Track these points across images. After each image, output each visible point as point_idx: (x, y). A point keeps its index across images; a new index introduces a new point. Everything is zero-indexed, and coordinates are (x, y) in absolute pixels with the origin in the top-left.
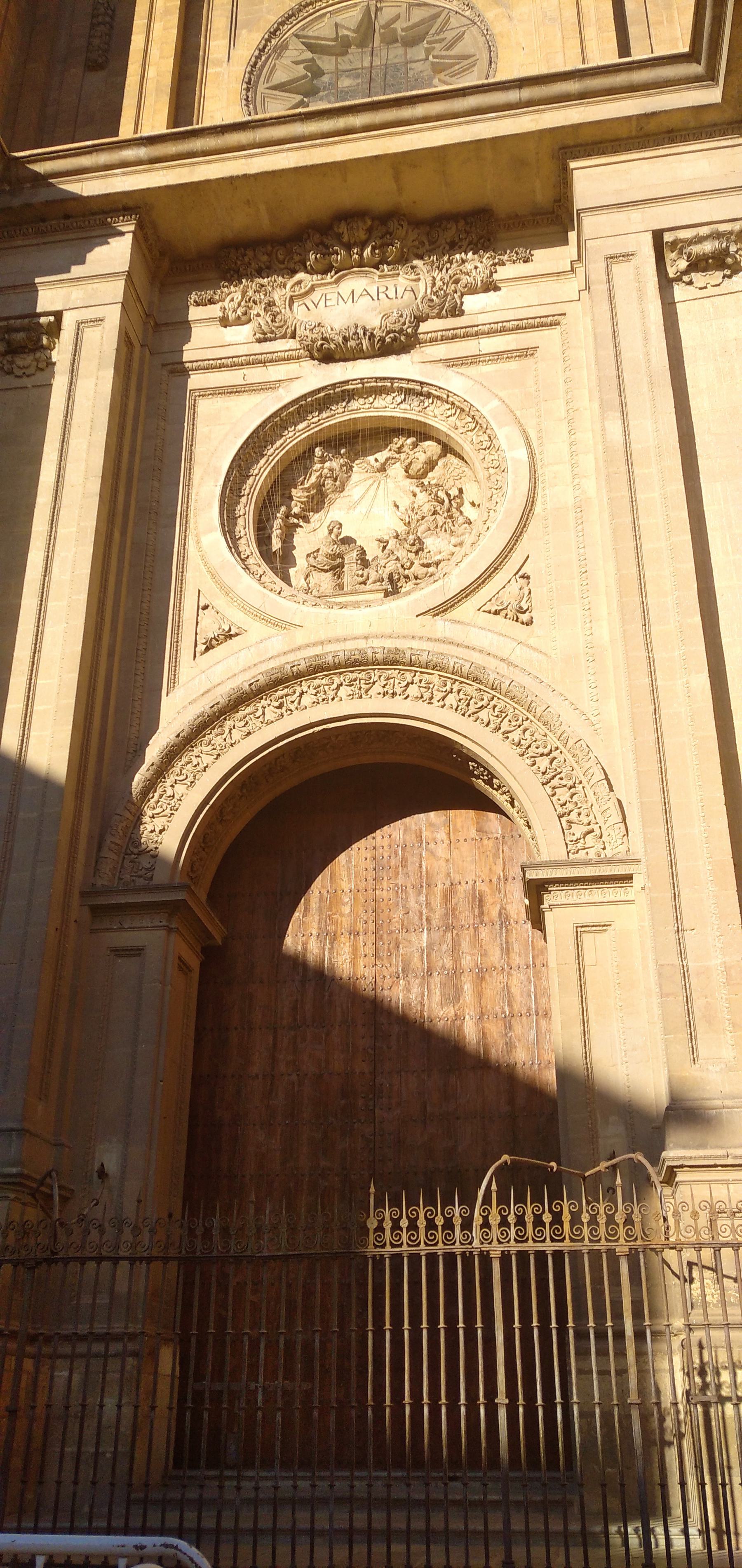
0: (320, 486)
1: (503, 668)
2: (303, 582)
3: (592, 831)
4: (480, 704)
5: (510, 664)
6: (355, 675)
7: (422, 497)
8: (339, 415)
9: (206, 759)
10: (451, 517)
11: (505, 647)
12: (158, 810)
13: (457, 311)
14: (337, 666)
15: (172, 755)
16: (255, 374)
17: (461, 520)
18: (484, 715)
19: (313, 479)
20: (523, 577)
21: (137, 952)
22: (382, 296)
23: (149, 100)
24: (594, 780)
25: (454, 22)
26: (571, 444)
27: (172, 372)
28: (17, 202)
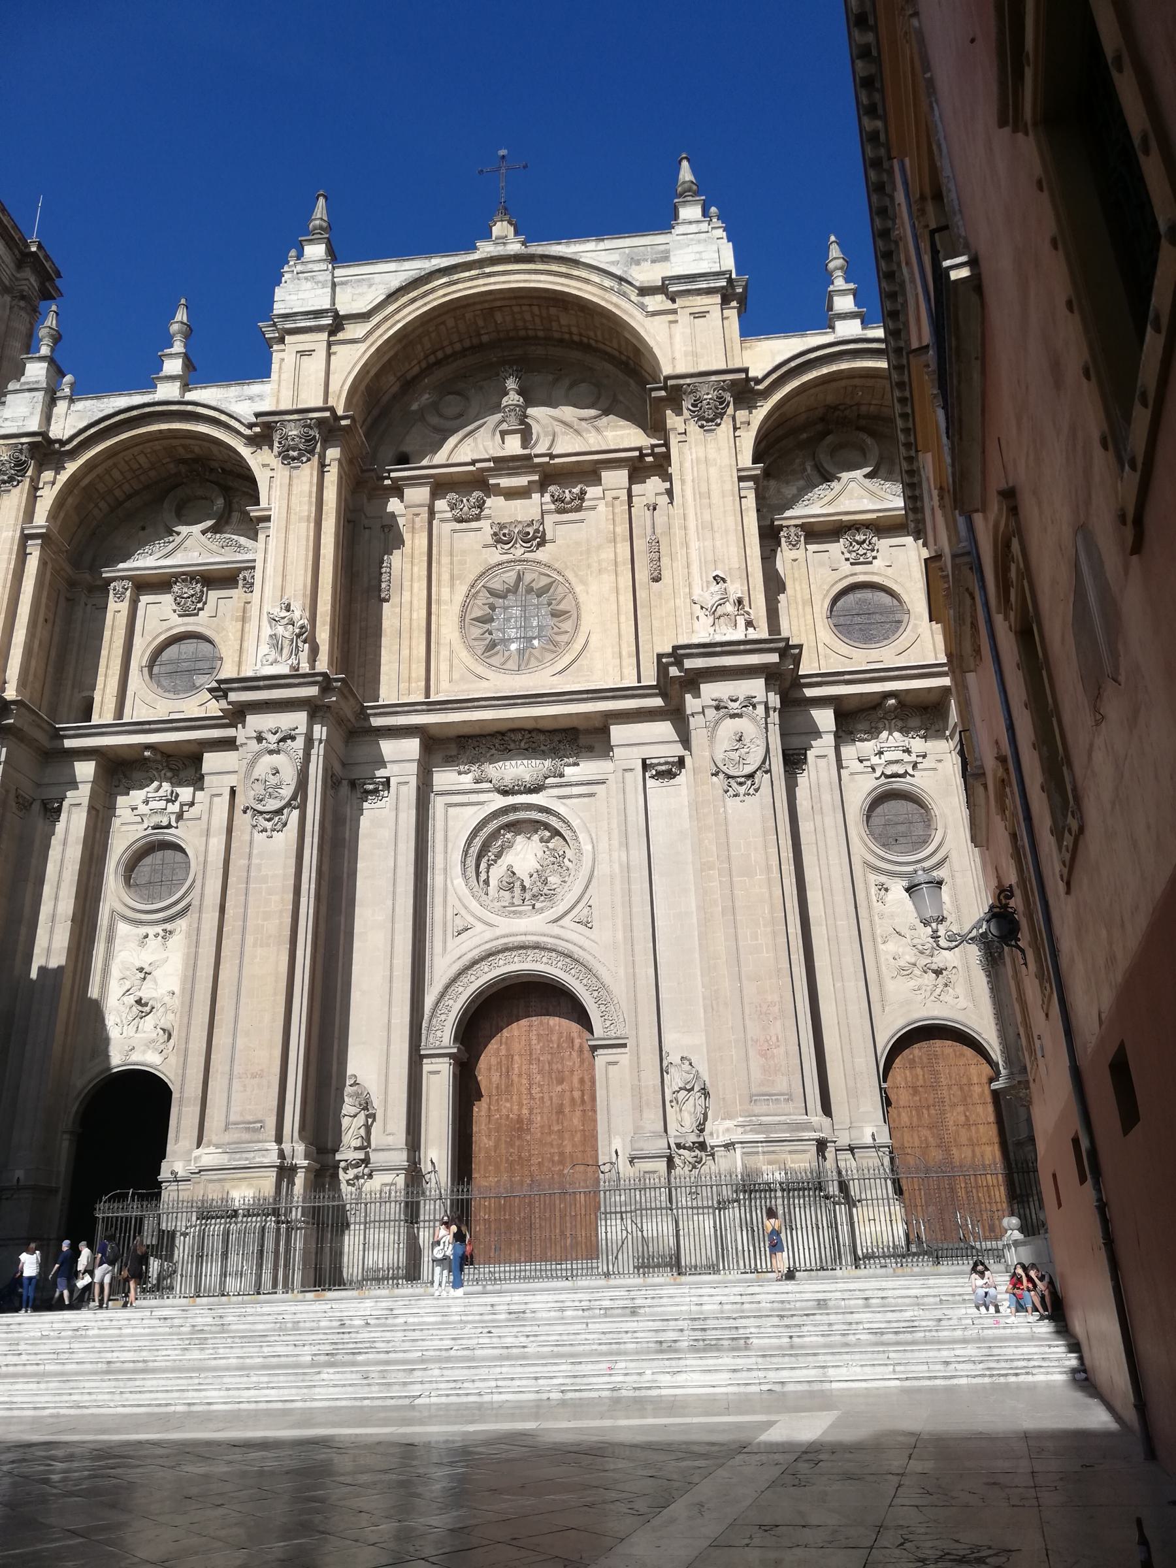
0: (502, 846)
1: (581, 952)
5: (584, 950)
8: (512, 817)
9: (461, 989)
13: (562, 775)
15: (447, 987)
16: (474, 798)
21: (438, 1072)
23: (415, 634)
25: (560, 589)
28: (366, 724)
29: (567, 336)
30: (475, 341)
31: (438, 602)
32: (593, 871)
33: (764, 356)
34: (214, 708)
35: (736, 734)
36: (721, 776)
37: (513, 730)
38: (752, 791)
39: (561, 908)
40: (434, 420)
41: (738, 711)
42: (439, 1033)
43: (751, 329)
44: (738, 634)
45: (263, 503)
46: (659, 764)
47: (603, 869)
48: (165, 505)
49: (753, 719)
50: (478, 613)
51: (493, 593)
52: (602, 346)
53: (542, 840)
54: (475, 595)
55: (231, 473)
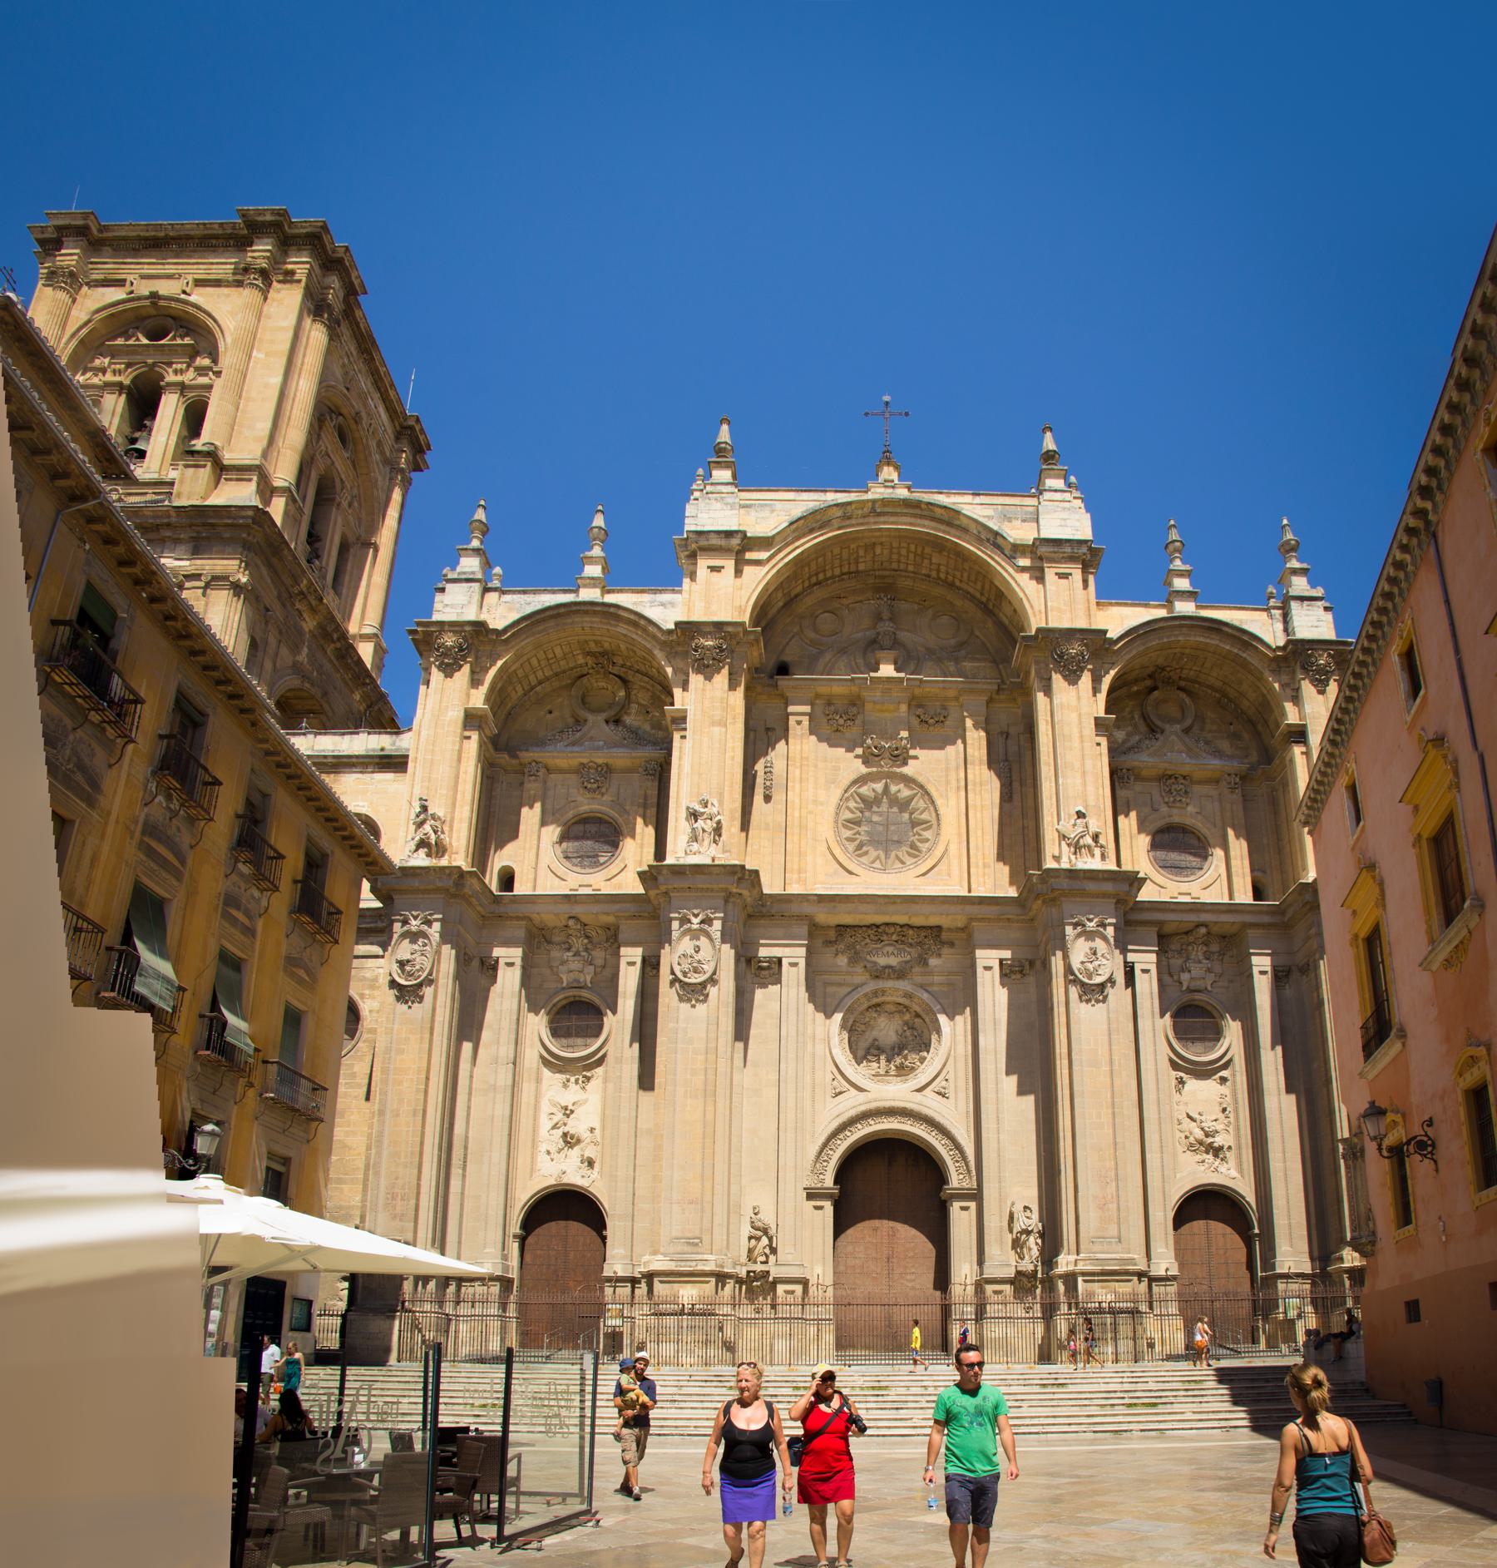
29: (934, 574)
30: (853, 568)
31: (815, 802)
33: (1118, 620)
34: (632, 885)
37: (887, 924)
40: (812, 635)
43: (1108, 595)
44: (1093, 863)
45: (678, 706)
48: (573, 693)
49: (1105, 938)
50: (849, 815)
51: (863, 799)
52: (964, 586)
54: (847, 799)
55: (630, 668)
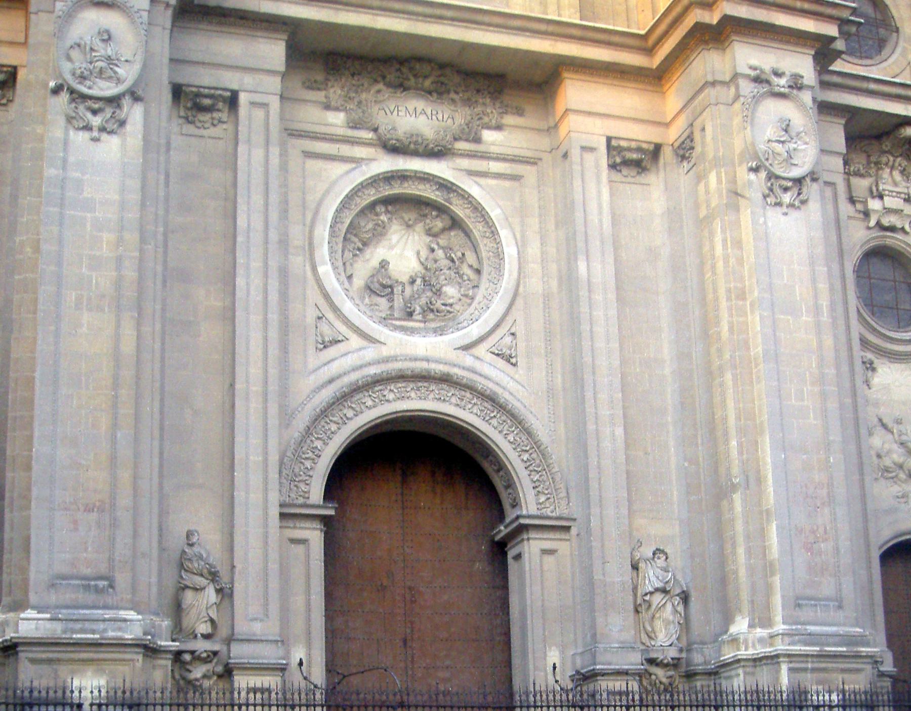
2: (367, 300)
3: (549, 498)
4: (492, 415)
6: (420, 384)
7: (440, 253)
8: (397, 189)
9: (334, 427)
10: (458, 273)
11: (505, 380)
12: (307, 456)
13: (478, 140)
14: (412, 377)
16: (346, 150)
17: (465, 278)
18: (494, 422)
19: (370, 226)
20: (513, 334)
21: (303, 541)
22: (434, 117)
24: (554, 470)
26: (542, 253)
27: (290, 135)
32: (518, 285)
35: (781, 120)
36: (763, 174)
37: (420, 59)
38: (797, 203)
39: (474, 331)
41: (786, 90)
42: (303, 487)
46: (629, 149)
47: (534, 284)
49: (802, 106)
53: (429, 232)
